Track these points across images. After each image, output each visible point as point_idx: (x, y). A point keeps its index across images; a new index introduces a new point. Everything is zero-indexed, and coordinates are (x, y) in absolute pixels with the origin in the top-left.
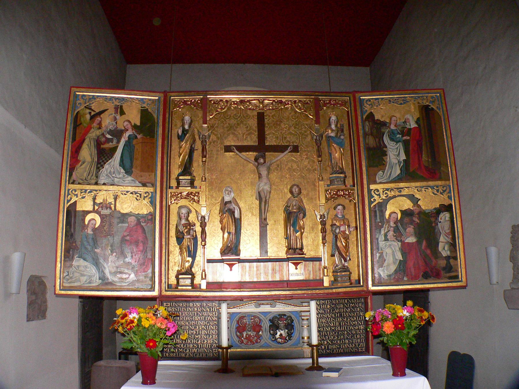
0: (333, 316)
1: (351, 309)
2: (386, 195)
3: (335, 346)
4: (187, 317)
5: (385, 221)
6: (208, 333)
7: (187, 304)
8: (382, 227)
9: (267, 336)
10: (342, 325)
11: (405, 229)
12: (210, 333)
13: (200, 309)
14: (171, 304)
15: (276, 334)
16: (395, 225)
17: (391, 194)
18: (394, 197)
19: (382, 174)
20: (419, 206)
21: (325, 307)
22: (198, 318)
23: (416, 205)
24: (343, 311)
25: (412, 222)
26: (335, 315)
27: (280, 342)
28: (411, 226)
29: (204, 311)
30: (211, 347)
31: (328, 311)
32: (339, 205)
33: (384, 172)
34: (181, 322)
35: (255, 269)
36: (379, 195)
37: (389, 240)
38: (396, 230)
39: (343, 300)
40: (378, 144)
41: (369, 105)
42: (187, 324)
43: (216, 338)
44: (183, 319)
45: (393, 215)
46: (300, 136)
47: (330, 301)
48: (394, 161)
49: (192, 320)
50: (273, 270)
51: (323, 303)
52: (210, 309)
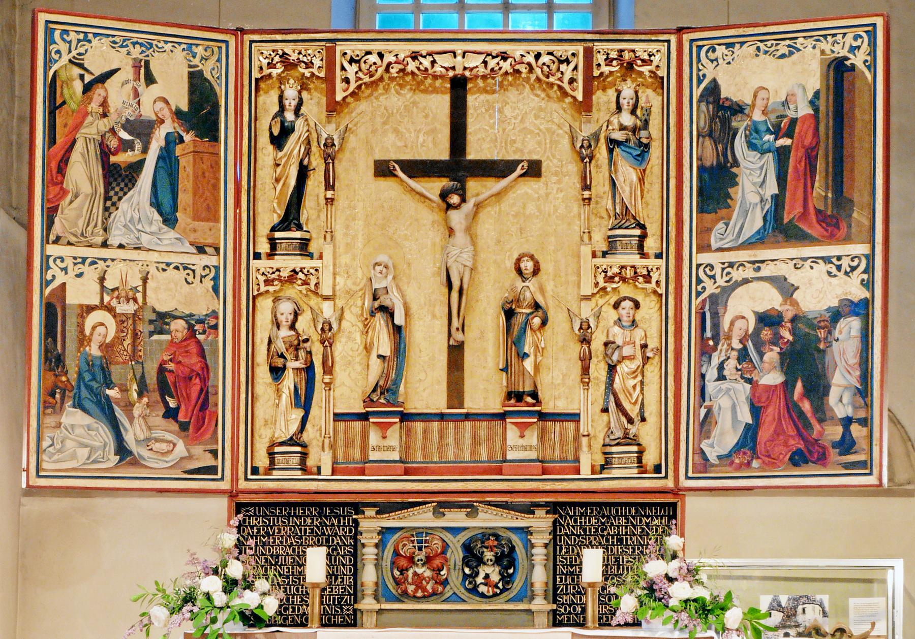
0: (604, 542)
1: (643, 529)
2: (727, 279)
3: (606, 608)
4: (290, 537)
5: (721, 334)
6: (333, 572)
7: (290, 509)
8: (715, 348)
9: (457, 579)
10: (623, 562)
11: (761, 355)
12: (337, 572)
13: (317, 520)
14: (255, 511)
15: (477, 574)
16: (740, 346)
17: (737, 275)
18: (746, 281)
19: (724, 229)
20: (795, 304)
21: (585, 522)
22: (312, 539)
23: (788, 302)
24: (626, 532)
25: (776, 339)
26: (607, 540)
27: (486, 593)
28: (775, 348)
29: (326, 525)
30: (339, 603)
31: (593, 530)
32: (624, 299)
33: (727, 225)
34: (276, 549)
35: (436, 435)
36: (713, 277)
37: (726, 379)
38: (743, 355)
39: (626, 509)
40: (722, 159)
41: (712, 61)
42: (290, 552)
43: (350, 582)
44: (282, 542)
45: (740, 324)
47: (596, 509)
48: (754, 199)
49: (301, 544)
51: (582, 514)
52: (339, 522)
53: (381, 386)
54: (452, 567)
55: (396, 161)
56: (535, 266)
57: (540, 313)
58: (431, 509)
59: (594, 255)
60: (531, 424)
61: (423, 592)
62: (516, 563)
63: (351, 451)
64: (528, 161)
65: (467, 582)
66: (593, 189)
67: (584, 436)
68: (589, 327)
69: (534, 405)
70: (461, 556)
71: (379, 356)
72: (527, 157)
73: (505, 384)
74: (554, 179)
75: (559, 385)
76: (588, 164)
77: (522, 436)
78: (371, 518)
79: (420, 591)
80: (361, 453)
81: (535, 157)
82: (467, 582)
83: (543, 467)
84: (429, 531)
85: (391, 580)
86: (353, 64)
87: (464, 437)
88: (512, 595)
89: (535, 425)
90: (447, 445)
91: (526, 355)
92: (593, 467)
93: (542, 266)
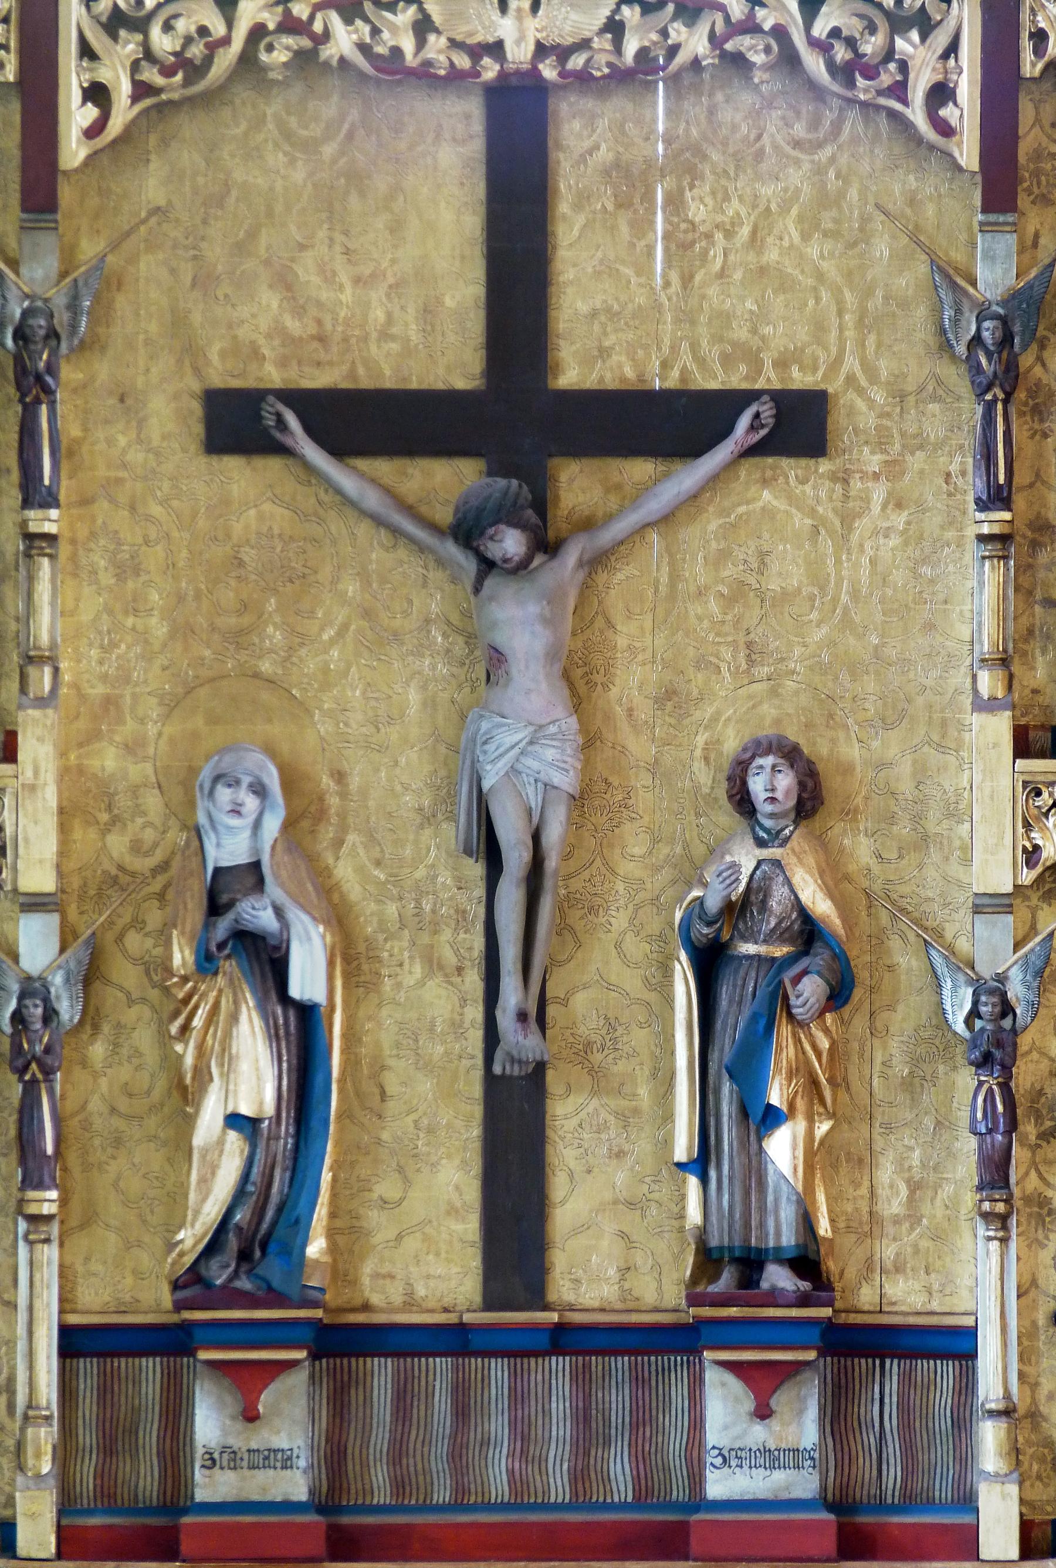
35: (442, 1403)
46: (848, 295)
50: (587, 1419)
53: (239, 1228)
55: (293, 398)
56: (802, 785)
57: (819, 958)
59: (1023, 748)
60: (797, 1367)
63: (125, 1468)
64: (780, 398)
66: (1019, 501)
67: (992, 1414)
68: (1006, 1009)
69: (804, 1300)
71: (234, 1120)
72: (769, 379)
73: (694, 1214)
74: (874, 461)
75: (897, 1221)
76: (1000, 406)
77: (763, 1413)
80: (163, 1470)
81: (800, 379)
83: (841, 1527)
86: (123, 33)
87: (546, 1413)
89: (807, 1374)
90: (485, 1443)
91: (771, 1118)
92: (1026, 1527)
93: (832, 783)
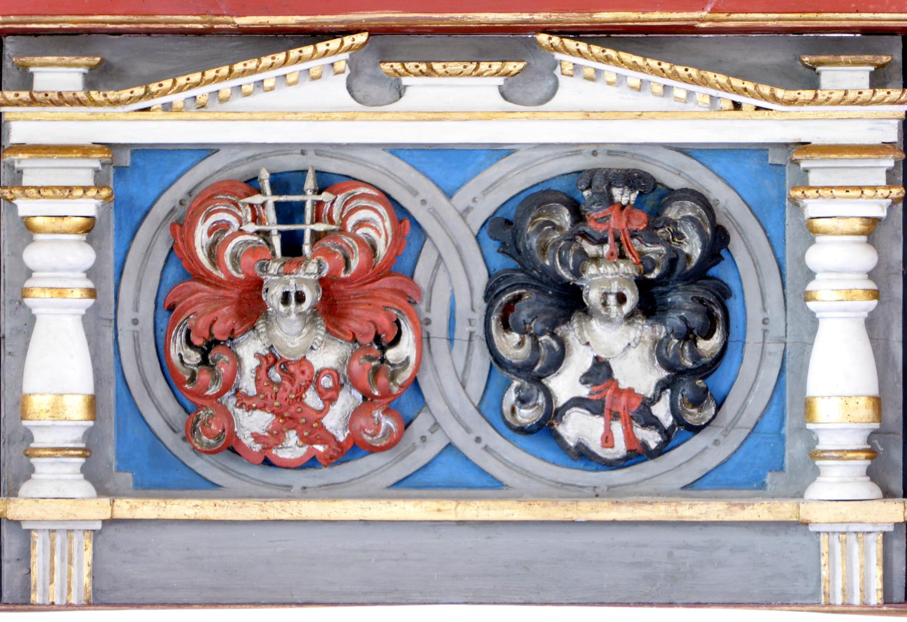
15: (557, 361)
27: (595, 445)
54: (439, 328)
58: (341, 60)
61: (307, 441)
62: (733, 305)
65: (511, 397)
70: (481, 279)
78: (61, 100)
79: (292, 437)
82: (511, 397)
84: (332, 166)
85: (160, 388)
88: (711, 461)
